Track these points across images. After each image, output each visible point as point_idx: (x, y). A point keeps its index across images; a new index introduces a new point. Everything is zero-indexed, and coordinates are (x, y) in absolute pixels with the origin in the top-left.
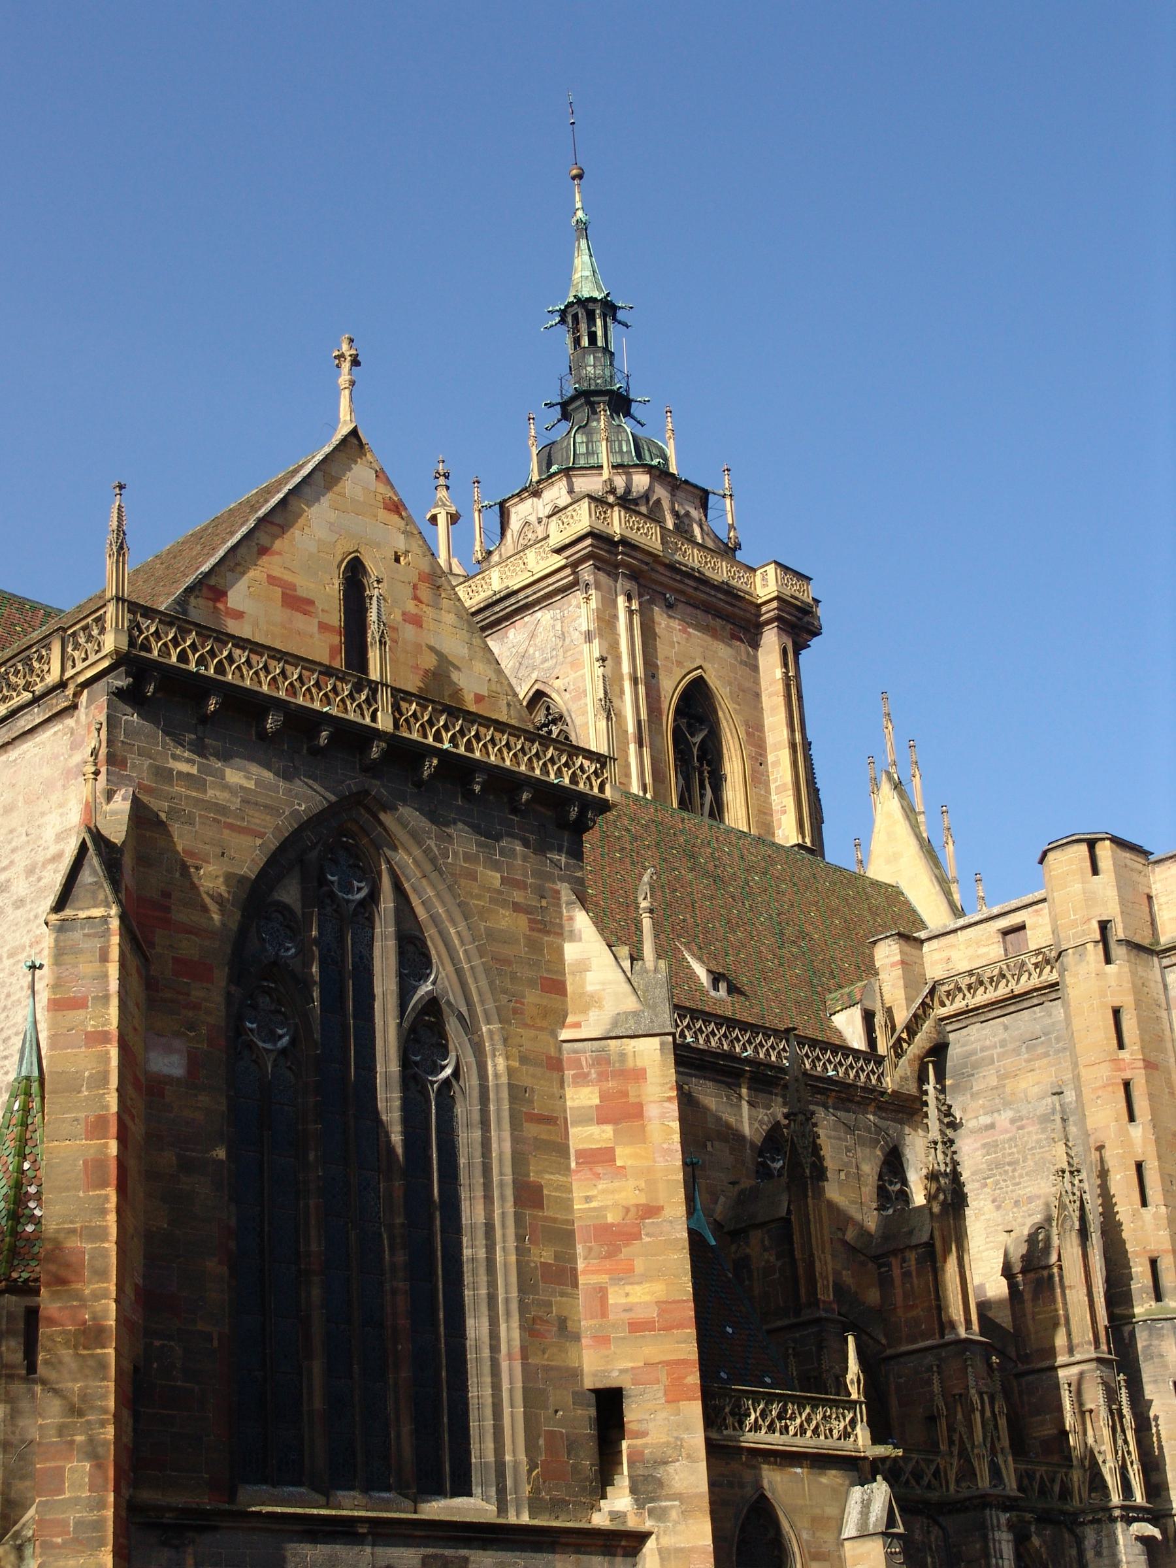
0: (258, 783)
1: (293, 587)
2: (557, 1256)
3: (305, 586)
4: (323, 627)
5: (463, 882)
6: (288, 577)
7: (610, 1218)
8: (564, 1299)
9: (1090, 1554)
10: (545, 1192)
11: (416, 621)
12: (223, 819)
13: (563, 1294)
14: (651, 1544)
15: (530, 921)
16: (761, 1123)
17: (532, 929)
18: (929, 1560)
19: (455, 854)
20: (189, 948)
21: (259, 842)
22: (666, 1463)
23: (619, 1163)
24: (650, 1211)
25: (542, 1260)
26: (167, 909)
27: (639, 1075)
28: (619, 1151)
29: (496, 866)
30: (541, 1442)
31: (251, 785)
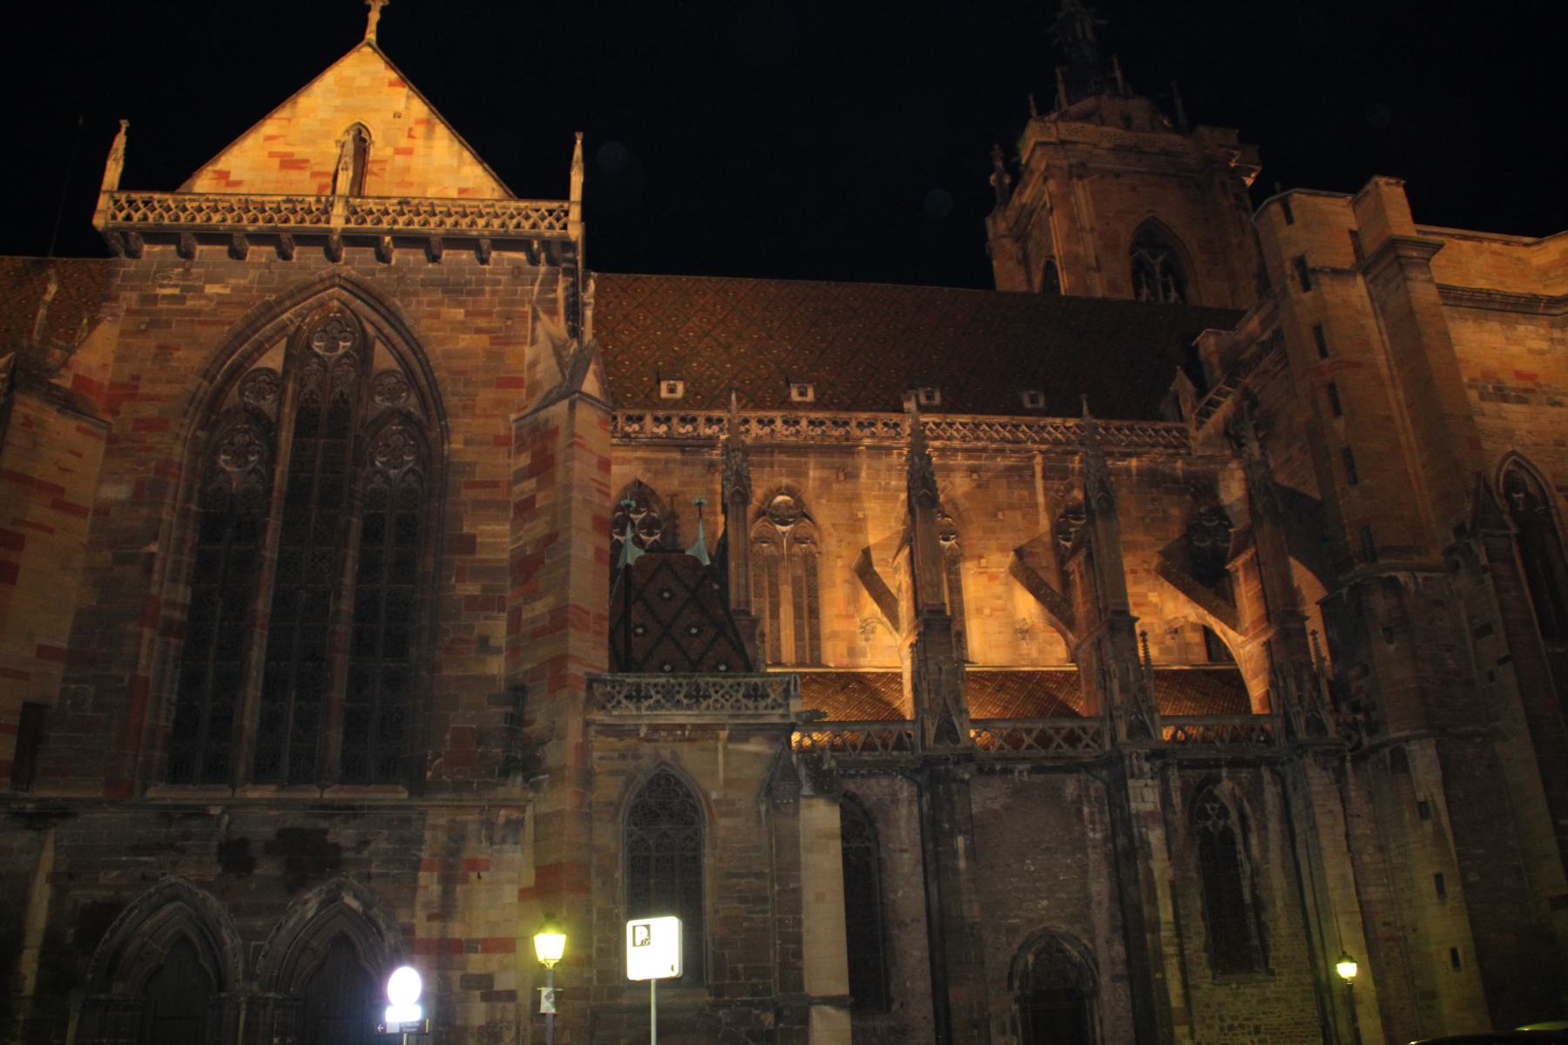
0: (233, 289)
1: (292, 154)
2: (484, 589)
3: (300, 151)
4: (315, 175)
5: (424, 322)
6: (288, 149)
7: (529, 551)
8: (488, 622)
9: (1290, 790)
10: (478, 540)
11: (408, 152)
12: (196, 319)
13: (486, 618)
14: (529, 812)
15: (491, 338)
16: (1057, 491)
17: (492, 344)
18: (1086, 810)
19: (419, 303)
20: (150, 411)
21: (227, 328)
22: (545, 743)
23: (537, 506)
24: (551, 538)
25: (467, 593)
26: (136, 387)
27: (554, 433)
28: (540, 496)
29: (461, 304)
30: (448, 737)
31: (228, 291)
